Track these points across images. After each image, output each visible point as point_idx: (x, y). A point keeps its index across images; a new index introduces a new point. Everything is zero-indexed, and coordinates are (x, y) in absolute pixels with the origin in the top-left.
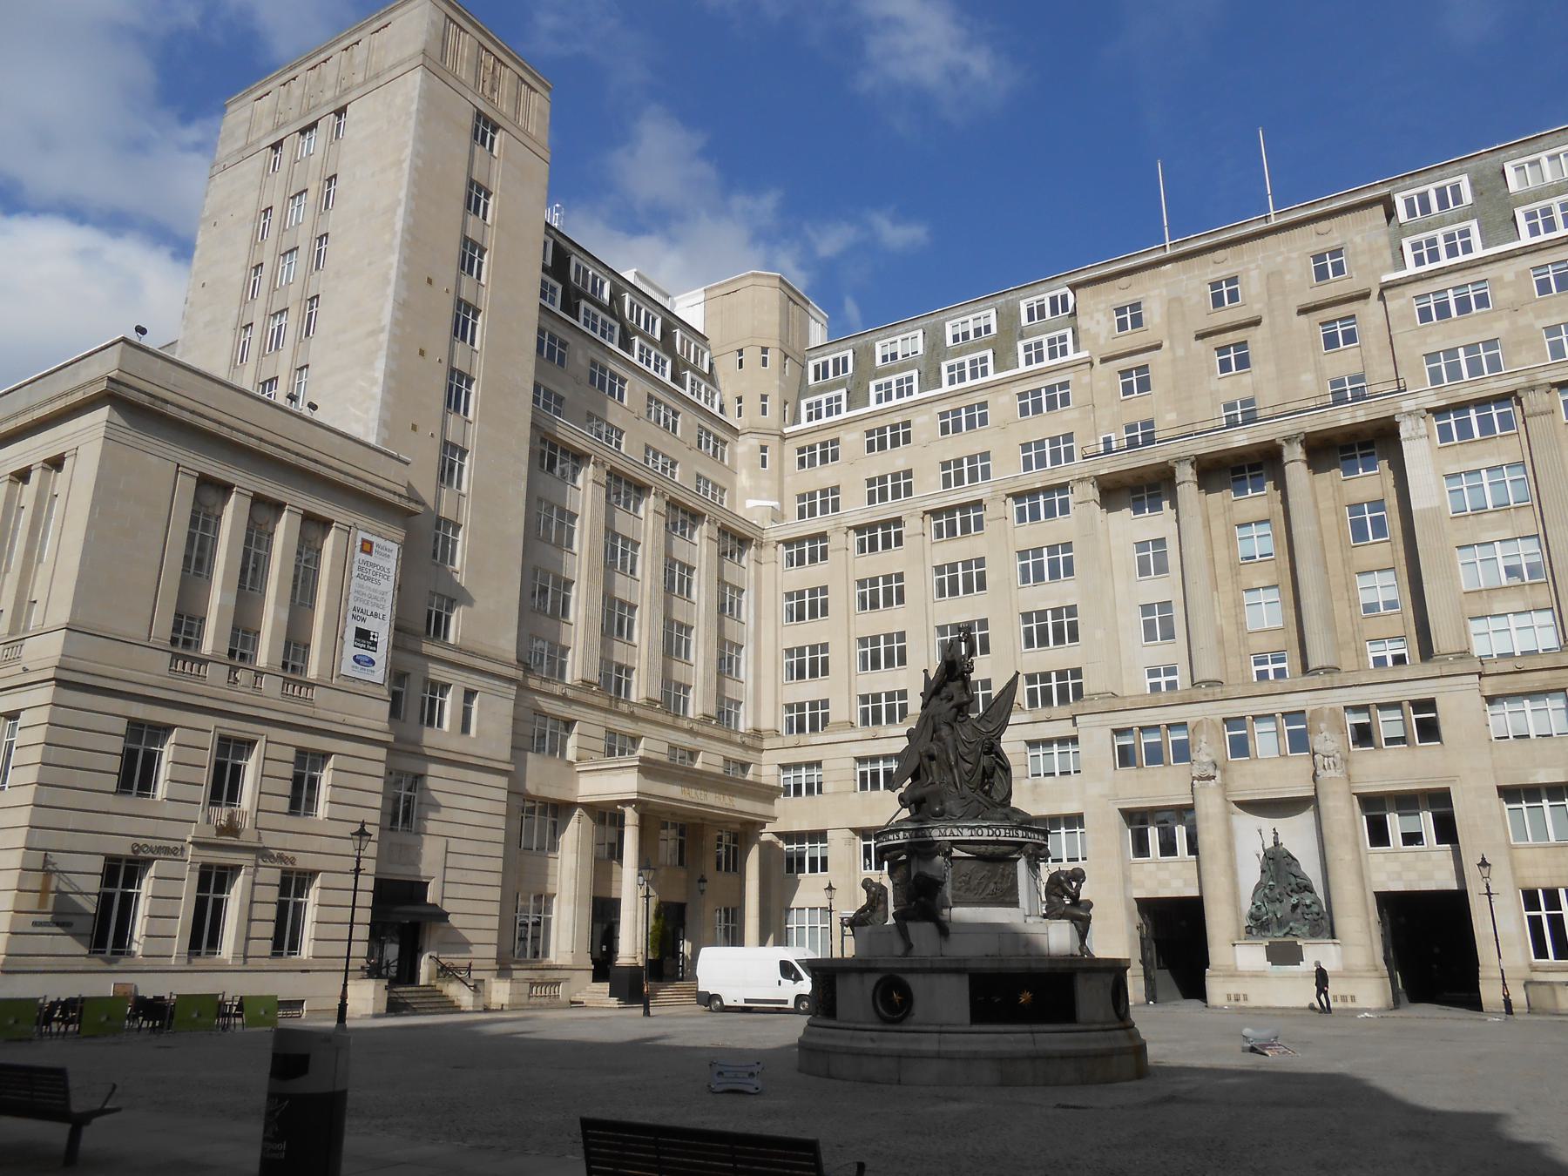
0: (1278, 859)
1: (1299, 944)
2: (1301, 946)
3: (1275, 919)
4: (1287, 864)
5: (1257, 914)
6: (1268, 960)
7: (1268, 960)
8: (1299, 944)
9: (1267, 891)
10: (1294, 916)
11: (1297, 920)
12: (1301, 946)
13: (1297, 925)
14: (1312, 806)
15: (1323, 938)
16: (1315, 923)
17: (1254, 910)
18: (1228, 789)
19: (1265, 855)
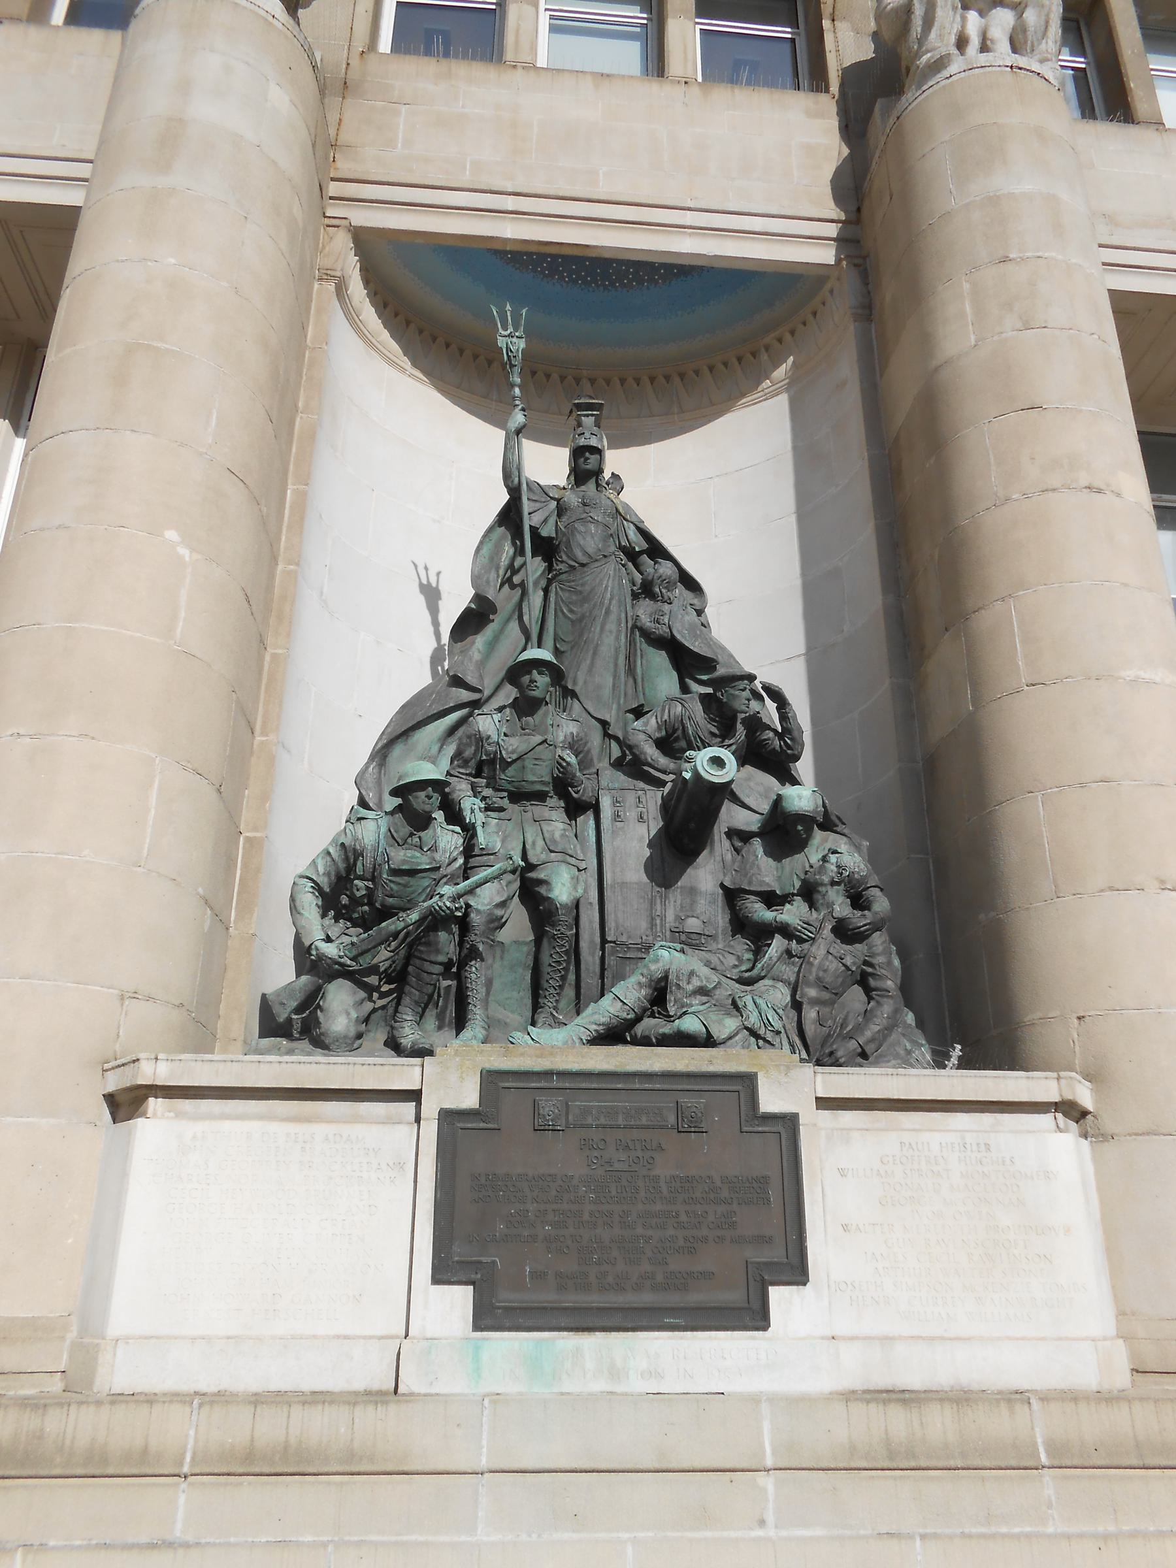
0: (588, 540)
1: (771, 1101)
2: (790, 1122)
3: (518, 924)
4: (646, 590)
5: (401, 857)
6: (442, 1274)
7: (442, 1274)
8: (771, 1101)
9: (488, 724)
10: (671, 908)
11: (688, 941)
12: (790, 1122)
13: (706, 976)
14: (781, 372)
15: (907, 1061)
16: (853, 954)
17: (372, 832)
18: (344, 166)
19: (510, 517)
